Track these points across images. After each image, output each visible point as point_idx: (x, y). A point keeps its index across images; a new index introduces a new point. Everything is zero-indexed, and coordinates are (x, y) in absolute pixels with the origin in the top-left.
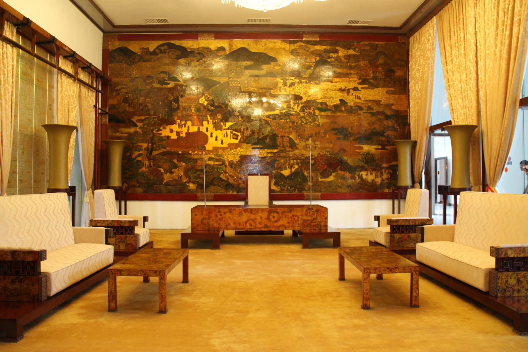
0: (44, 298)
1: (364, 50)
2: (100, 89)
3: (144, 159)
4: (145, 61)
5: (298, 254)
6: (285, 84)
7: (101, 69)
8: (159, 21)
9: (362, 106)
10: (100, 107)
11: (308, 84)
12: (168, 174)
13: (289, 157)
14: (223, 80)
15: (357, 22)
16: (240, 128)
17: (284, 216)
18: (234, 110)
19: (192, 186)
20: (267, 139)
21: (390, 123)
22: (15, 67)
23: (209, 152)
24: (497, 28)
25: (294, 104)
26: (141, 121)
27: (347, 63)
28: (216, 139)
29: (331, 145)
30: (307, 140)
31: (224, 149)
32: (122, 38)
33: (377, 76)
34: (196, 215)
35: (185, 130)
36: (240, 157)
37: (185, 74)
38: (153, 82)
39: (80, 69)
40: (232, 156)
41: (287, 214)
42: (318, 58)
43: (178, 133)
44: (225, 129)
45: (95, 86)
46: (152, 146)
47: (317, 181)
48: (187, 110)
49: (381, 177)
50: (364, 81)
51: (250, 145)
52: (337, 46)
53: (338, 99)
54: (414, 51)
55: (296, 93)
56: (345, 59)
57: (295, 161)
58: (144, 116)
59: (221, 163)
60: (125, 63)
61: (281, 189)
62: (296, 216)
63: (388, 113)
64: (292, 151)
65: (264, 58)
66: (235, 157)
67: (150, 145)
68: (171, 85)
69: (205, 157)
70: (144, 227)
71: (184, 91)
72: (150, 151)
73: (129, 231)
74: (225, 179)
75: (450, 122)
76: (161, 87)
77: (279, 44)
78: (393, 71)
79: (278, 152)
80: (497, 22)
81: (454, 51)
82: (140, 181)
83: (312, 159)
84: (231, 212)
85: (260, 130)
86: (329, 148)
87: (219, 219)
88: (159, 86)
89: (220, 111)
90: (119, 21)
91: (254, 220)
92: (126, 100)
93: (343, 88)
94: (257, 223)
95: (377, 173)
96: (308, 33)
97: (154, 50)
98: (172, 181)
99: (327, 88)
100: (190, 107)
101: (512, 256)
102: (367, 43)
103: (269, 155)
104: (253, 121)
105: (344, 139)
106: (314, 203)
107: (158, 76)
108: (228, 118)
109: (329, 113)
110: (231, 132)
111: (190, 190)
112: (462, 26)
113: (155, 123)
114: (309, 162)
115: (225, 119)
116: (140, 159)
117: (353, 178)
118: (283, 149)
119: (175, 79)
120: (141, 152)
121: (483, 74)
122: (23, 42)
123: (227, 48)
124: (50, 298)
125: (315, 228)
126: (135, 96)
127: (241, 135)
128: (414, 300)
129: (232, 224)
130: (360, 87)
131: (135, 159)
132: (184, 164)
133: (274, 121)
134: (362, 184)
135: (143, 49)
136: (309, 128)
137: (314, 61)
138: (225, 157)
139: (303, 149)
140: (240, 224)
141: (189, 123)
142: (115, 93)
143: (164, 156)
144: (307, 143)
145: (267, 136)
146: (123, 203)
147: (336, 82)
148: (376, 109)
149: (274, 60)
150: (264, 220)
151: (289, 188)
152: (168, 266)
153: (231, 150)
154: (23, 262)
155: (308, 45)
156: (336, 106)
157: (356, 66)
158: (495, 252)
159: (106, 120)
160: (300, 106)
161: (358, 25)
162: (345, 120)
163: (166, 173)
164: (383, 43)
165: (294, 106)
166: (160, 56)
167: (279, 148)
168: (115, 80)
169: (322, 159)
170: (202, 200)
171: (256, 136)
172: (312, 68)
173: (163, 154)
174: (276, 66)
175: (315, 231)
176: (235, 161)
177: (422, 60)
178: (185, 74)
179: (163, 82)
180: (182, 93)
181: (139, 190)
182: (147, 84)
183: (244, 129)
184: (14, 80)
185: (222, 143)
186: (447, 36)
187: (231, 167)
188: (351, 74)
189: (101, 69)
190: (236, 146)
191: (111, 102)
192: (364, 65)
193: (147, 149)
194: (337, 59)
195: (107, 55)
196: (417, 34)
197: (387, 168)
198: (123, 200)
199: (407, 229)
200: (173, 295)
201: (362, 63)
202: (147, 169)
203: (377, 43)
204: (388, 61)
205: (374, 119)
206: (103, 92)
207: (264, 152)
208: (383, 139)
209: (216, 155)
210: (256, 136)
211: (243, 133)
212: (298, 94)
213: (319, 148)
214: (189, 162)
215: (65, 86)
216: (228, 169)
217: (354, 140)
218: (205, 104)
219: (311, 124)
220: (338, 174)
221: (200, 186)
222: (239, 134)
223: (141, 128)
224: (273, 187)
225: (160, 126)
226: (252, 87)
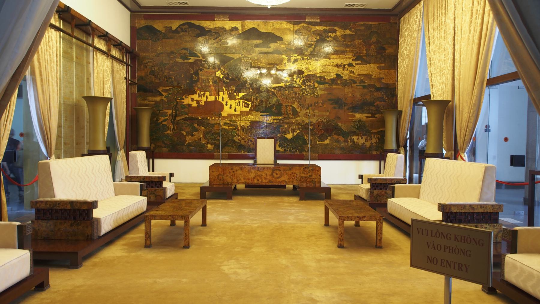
0: (96, 237)
1: (359, 30)
2: (130, 63)
4: (168, 38)
5: (295, 204)
6: (289, 60)
7: (129, 46)
8: (180, 3)
13: (292, 123)
14: (236, 56)
15: (354, 5)
18: (245, 82)
19: (210, 146)
21: (379, 94)
22: (58, 48)
23: (225, 118)
24: (472, 16)
25: (297, 79)
26: (166, 91)
27: (344, 41)
28: (231, 108)
29: (328, 114)
31: (237, 115)
32: (147, 17)
34: (213, 172)
35: (204, 99)
37: (204, 48)
38: (176, 57)
39: (112, 46)
40: (244, 122)
42: (318, 38)
43: (198, 102)
45: (125, 61)
46: (176, 112)
48: (206, 82)
50: (358, 58)
51: (259, 113)
53: (335, 74)
54: (404, 31)
56: (342, 38)
57: (297, 126)
60: (151, 39)
63: (378, 85)
65: (272, 37)
69: (222, 123)
70: (170, 182)
71: (203, 65)
72: (174, 116)
73: (158, 185)
75: (429, 97)
77: (285, 25)
78: (384, 49)
80: (472, 10)
81: (436, 33)
85: (267, 100)
87: (232, 175)
88: (181, 61)
89: (235, 83)
91: (260, 176)
92: (152, 73)
100: (208, 80)
101: (455, 211)
102: (362, 23)
103: (275, 121)
104: (261, 92)
105: (339, 108)
106: (312, 162)
107: (180, 52)
109: (327, 86)
110: (243, 102)
111: (208, 150)
112: (444, 11)
113: (178, 92)
116: (165, 123)
117: (346, 141)
119: (195, 55)
121: (458, 55)
122: (64, 25)
123: (240, 28)
124: (100, 237)
125: (310, 184)
128: (378, 242)
129: (242, 179)
130: (354, 63)
132: (203, 128)
135: (167, 27)
136: (309, 99)
139: (304, 117)
140: (249, 179)
141: (207, 93)
142: (142, 66)
144: (307, 111)
146: (151, 161)
148: (367, 82)
149: (281, 39)
150: (268, 176)
152: (191, 212)
153: (243, 117)
154: (79, 210)
155: (310, 26)
156: (333, 80)
157: (351, 44)
158: (442, 207)
159: (135, 89)
161: (354, 7)
162: (339, 91)
164: (377, 23)
165: (297, 79)
166: (181, 34)
168: (142, 54)
171: (264, 105)
173: (185, 119)
174: (282, 44)
175: (310, 186)
177: (409, 40)
178: (204, 48)
179: (184, 58)
181: (165, 150)
184: (58, 59)
185: (235, 111)
186: (431, 19)
187: (243, 131)
189: (129, 46)
190: (247, 113)
193: (171, 115)
195: (135, 32)
196: (407, 15)
199: (385, 186)
200: (194, 235)
201: (356, 42)
202: (171, 132)
203: (371, 23)
204: (380, 40)
205: (365, 91)
208: (373, 108)
209: (231, 121)
210: (264, 105)
211: (253, 103)
213: (317, 116)
215: (100, 62)
217: (348, 109)
220: (333, 138)
221: (217, 147)
222: (250, 103)
224: (278, 148)
226: (261, 63)
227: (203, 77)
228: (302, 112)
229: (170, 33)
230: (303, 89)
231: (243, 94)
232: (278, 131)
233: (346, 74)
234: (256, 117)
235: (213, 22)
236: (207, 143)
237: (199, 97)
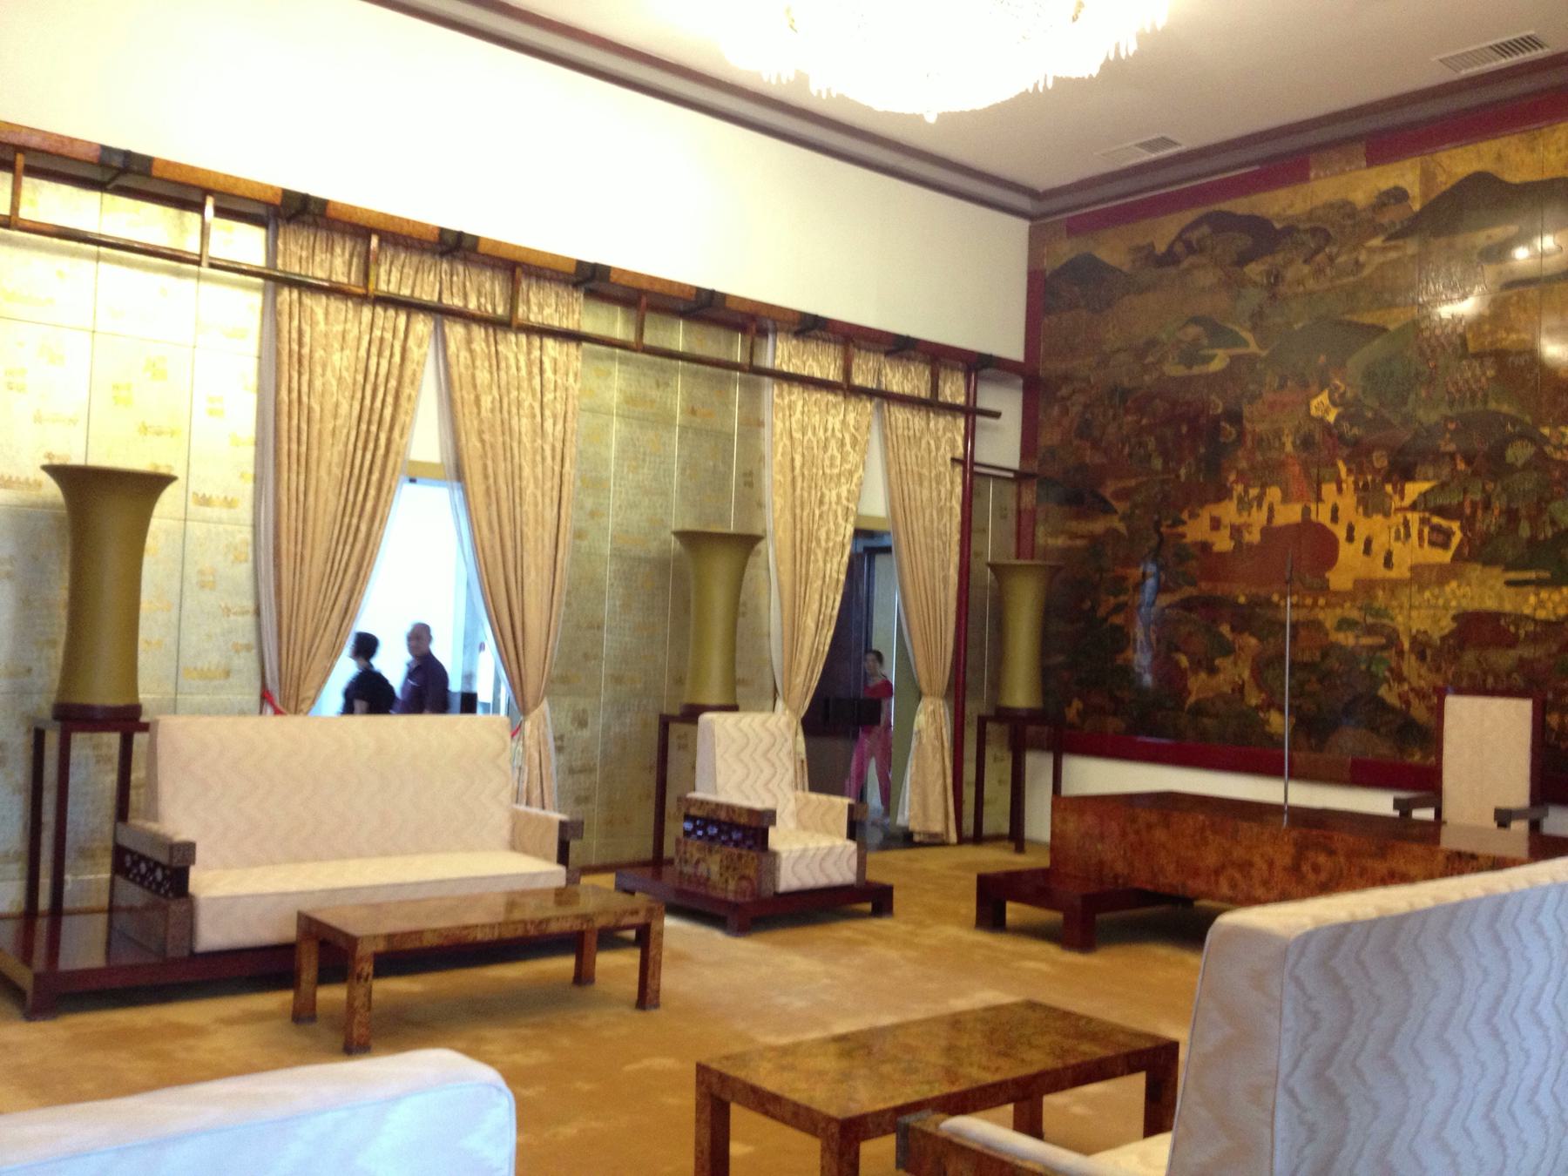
12: (1203, 675)
16: (1461, 504)
23: (1342, 596)
26: (1123, 494)
31: (1393, 586)
32: (1077, 227)
35: (1259, 518)
36: (1455, 618)
43: (1236, 531)
44: (1398, 510)
51: (1497, 571)
59: (1384, 641)
66: (1436, 620)
69: (1329, 618)
82: (1118, 693)
84: (1168, 826)
100: (1278, 434)
104: (1511, 469)
110: (1423, 521)
115: (1403, 472)
116: (1118, 620)
120: (1123, 598)
126: (1111, 413)
127: (1462, 528)
131: (1106, 619)
132: (1253, 641)
135: (1139, 249)
138: (1400, 619)
141: (1274, 493)
142: (1056, 411)
153: (1422, 589)
163: (1196, 672)
166: (1185, 264)
176: (1436, 636)
180: (1251, 387)
183: (1474, 505)
185: (1388, 562)
187: (1422, 657)
207: (1556, 597)
209: (1367, 609)
210: (1525, 531)
211: (1468, 526)
216: (1410, 666)
218: (1331, 418)
222: (1455, 526)
225: (1181, 511)
231: (1424, 486)
234: (1486, 591)
235: (1303, 189)
237: (1240, 511)
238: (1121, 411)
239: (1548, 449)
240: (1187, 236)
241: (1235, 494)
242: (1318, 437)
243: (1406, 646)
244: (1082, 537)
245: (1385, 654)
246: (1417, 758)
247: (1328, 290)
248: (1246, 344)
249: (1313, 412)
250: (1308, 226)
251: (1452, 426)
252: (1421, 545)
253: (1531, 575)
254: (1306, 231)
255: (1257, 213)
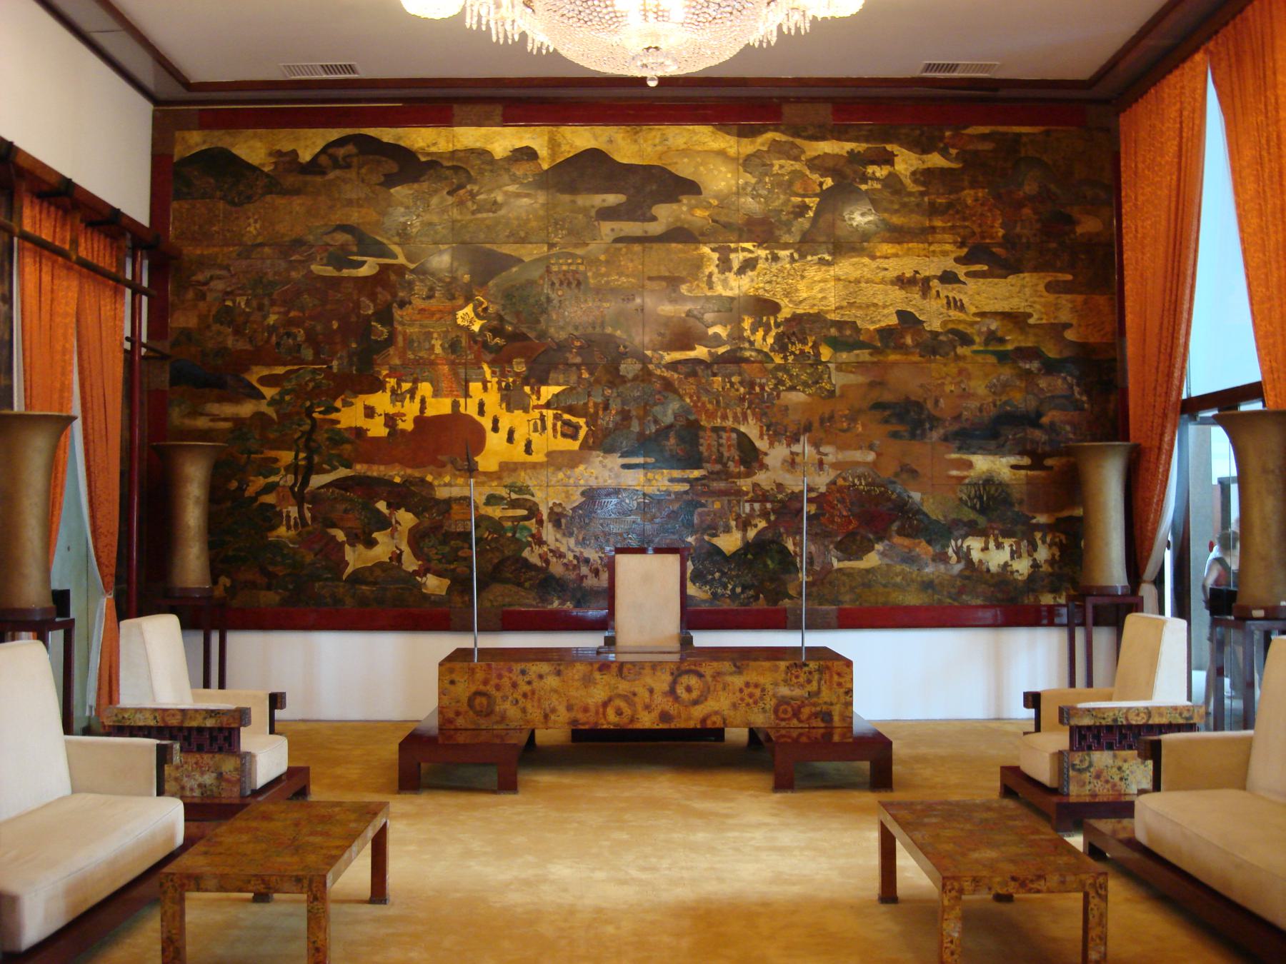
2: (145, 283)
3: (282, 499)
6: (725, 265)
8: (326, 69)
9: (969, 330)
10: (144, 339)
11: (796, 265)
12: (360, 547)
13: (739, 493)
15: (953, 67)
16: (586, 404)
17: (720, 686)
19: (433, 584)
20: (667, 438)
21: (1057, 384)
25: (754, 331)
27: (922, 194)
28: (510, 439)
29: (871, 457)
30: (795, 439)
31: (534, 466)
32: (211, 121)
33: (1019, 236)
34: (452, 682)
35: (411, 409)
36: (583, 494)
38: (311, 259)
41: (729, 679)
43: (390, 420)
46: (309, 459)
47: (827, 569)
49: (1030, 555)
52: (891, 142)
53: (892, 310)
55: (761, 292)
56: (916, 181)
57: (757, 506)
58: (285, 364)
59: (525, 512)
61: (714, 594)
62: (756, 686)
63: (1051, 352)
64: (749, 474)
66: (568, 496)
67: (302, 455)
68: (368, 268)
74: (538, 562)
76: (335, 274)
77: (705, 137)
78: (1071, 221)
79: (704, 477)
82: (271, 568)
83: (809, 500)
84: (559, 673)
86: (865, 464)
87: (525, 695)
88: (329, 271)
90: (201, 68)
91: (629, 698)
92: (226, 316)
93: (909, 274)
94: (639, 707)
95: (1018, 544)
96: (799, 100)
97: (315, 158)
98: (370, 569)
99: (857, 274)
100: (429, 336)
102: (985, 130)
104: (623, 380)
105: (913, 436)
106: (815, 639)
107: (327, 239)
108: (548, 373)
109: (864, 355)
110: (556, 417)
111: (426, 597)
114: (802, 509)
115: (539, 377)
116: (270, 499)
117: (942, 558)
118: (718, 467)
119: (382, 251)
126: (254, 303)
127: (587, 423)
130: (961, 271)
131: (254, 499)
132: (410, 515)
133: (691, 380)
134: (967, 578)
135: (279, 153)
137: (818, 190)
141: (425, 388)
142: (190, 295)
143: (346, 490)
144: (796, 448)
145: (670, 427)
146: (215, 638)
147: (886, 258)
148: (1013, 341)
149: (691, 187)
150: (658, 698)
151: (738, 590)
155: (798, 141)
157: (950, 205)
159: (162, 378)
160: (773, 333)
161: (956, 75)
165: (754, 331)
166: (332, 175)
167: (708, 465)
168: (192, 251)
169: (842, 501)
170: (466, 628)
172: (811, 214)
173: (339, 484)
174: (697, 207)
176: (569, 507)
179: (341, 259)
180: (401, 294)
181: (270, 598)
182: (292, 265)
183: (596, 405)
185: (528, 449)
187: (557, 524)
188: (933, 229)
191: (182, 320)
192: (976, 200)
193: (293, 468)
194: (893, 183)
195: (167, 175)
197: (1045, 528)
198: (215, 628)
201: (968, 195)
202: (292, 533)
203: (1017, 129)
204: (1052, 187)
205: (1006, 372)
206: (154, 293)
208: (1038, 435)
209: (512, 488)
210: (635, 427)
211: (592, 421)
212: (767, 295)
213: (834, 466)
214: (425, 510)
216: (549, 533)
217: (945, 439)
218: (476, 327)
219: (808, 391)
221: (460, 584)
222: (582, 421)
223: (273, 402)
224: (692, 590)
225: (335, 399)
226: (620, 274)
227: (409, 330)
228: (776, 454)
229: (293, 175)
230: (779, 368)
232: (690, 527)
233: (933, 314)
234: (604, 470)
235: (444, 131)
236: (424, 571)
238: (266, 302)
239: (651, 367)
240: (331, 151)
241: (388, 386)
242: (464, 342)
243: (545, 517)
244: (226, 420)
245: (526, 523)
246: (556, 604)
247: (471, 221)
248: (395, 257)
249: (460, 321)
250: (450, 164)
251: (578, 344)
252: (555, 437)
253: (640, 460)
254: (448, 168)
255: (402, 144)
